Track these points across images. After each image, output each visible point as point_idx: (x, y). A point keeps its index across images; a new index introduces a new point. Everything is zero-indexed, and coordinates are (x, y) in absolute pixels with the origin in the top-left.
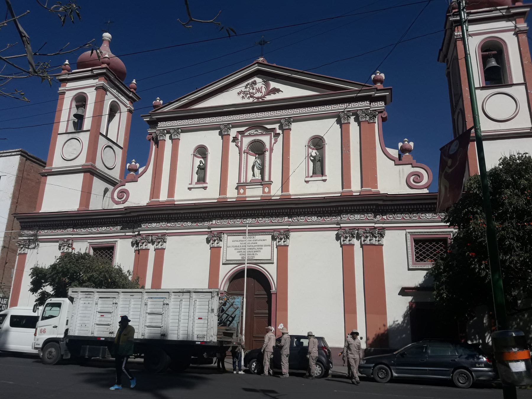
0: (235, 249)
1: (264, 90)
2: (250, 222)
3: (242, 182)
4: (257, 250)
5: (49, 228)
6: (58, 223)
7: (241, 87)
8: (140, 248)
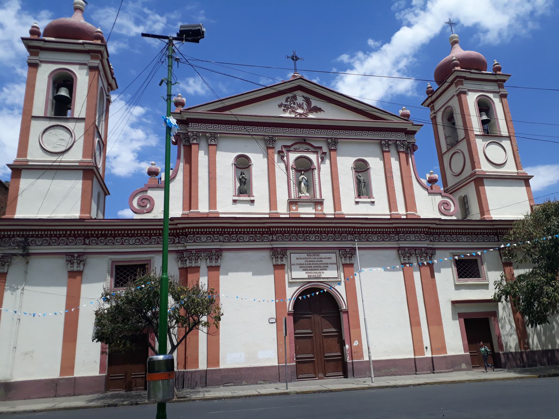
0: (300, 267)
1: (305, 107)
2: (312, 240)
3: (293, 198)
4: (323, 268)
5: (44, 238)
6: (61, 233)
7: (282, 99)
8: (188, 266)
